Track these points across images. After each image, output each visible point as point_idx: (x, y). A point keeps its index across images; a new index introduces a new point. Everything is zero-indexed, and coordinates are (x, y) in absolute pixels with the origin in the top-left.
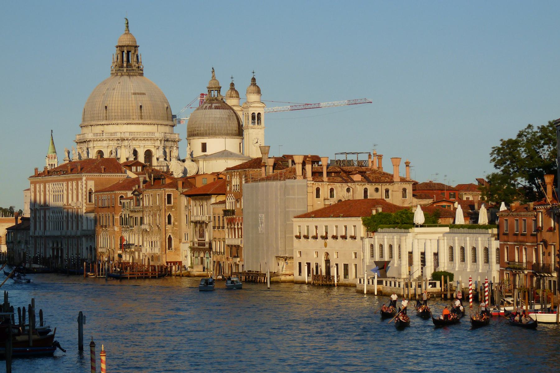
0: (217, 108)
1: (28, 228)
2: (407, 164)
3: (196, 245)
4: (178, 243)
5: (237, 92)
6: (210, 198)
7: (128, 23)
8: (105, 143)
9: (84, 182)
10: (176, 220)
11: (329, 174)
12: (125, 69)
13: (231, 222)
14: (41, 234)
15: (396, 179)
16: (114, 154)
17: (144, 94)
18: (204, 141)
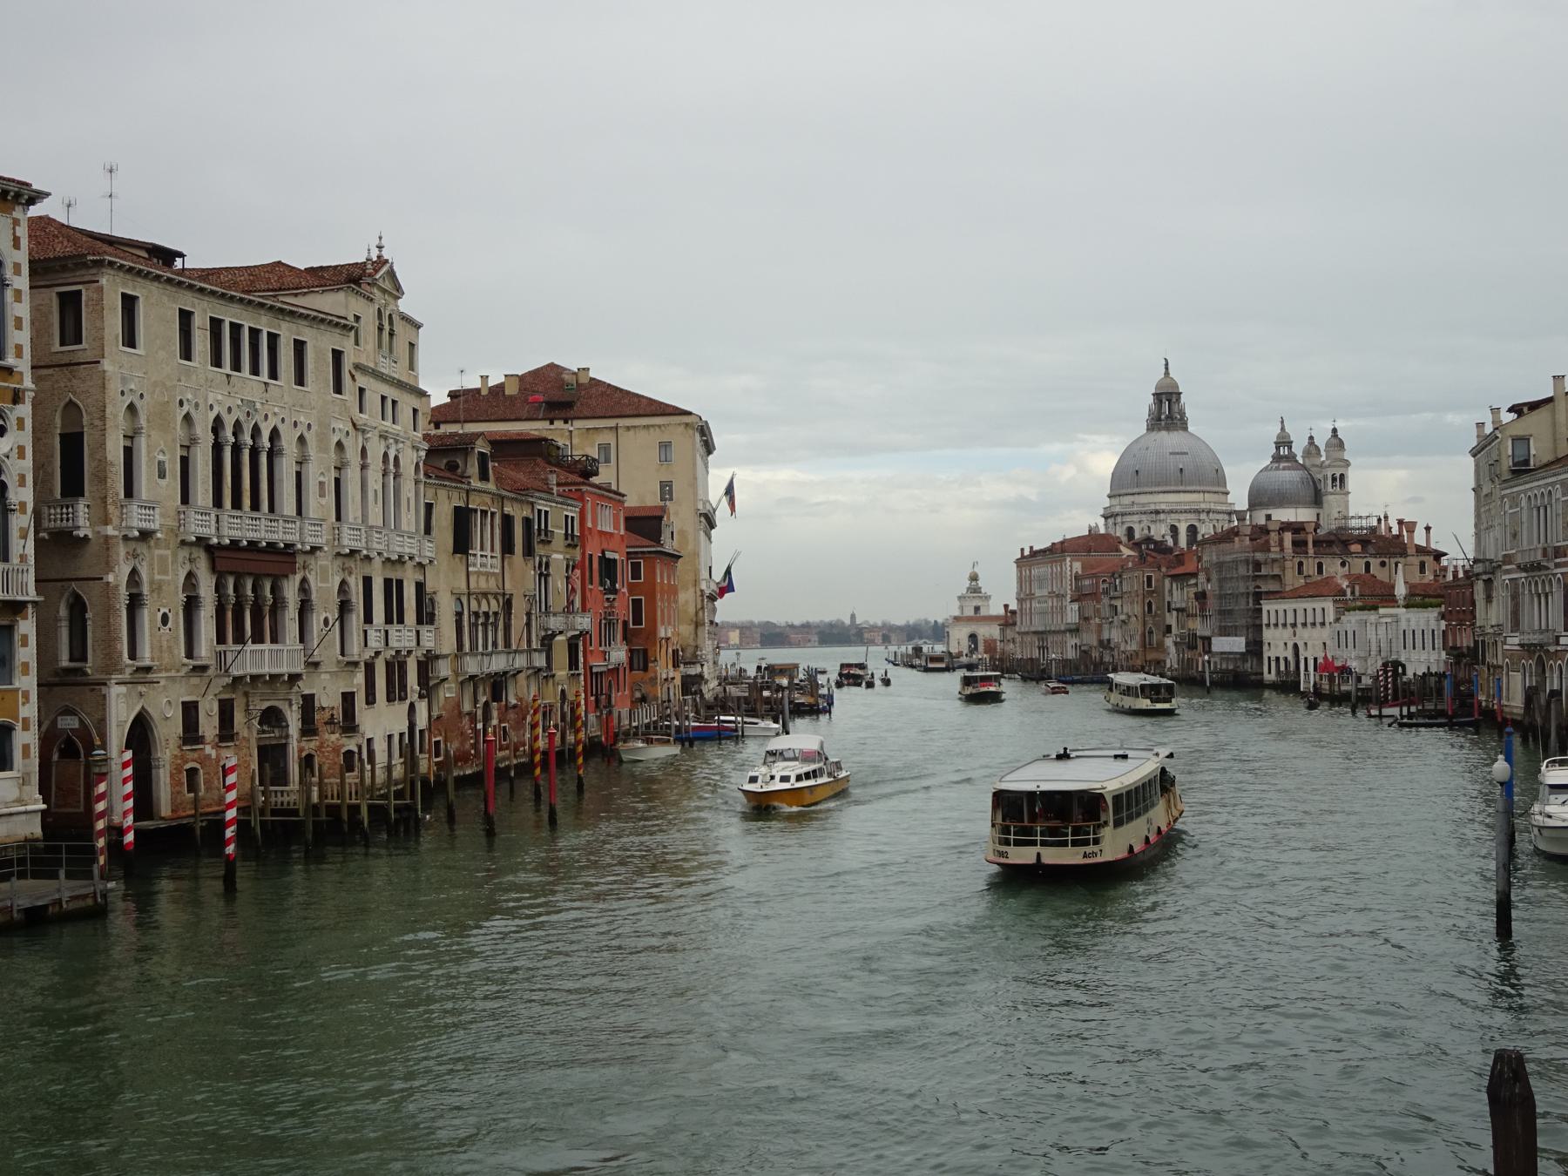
0: (1288, 468)
1: (1014, 624)
2: (1428, 529)
3: (1178, 640)
4: (1160, 637)
5: (1317, 447)
6: (1188, 580)
7: (1167, 365)
8: (1136, 518)
9: (1069, 564)
10: (1158, 608)
11: (1316, 543)
12: (1163, 423)
13: (1203, 609)
14: (1027, 630)
15: (1411, 551)
16: (1146, 531)
17: (1186, 453)
18: (1269, 512)
